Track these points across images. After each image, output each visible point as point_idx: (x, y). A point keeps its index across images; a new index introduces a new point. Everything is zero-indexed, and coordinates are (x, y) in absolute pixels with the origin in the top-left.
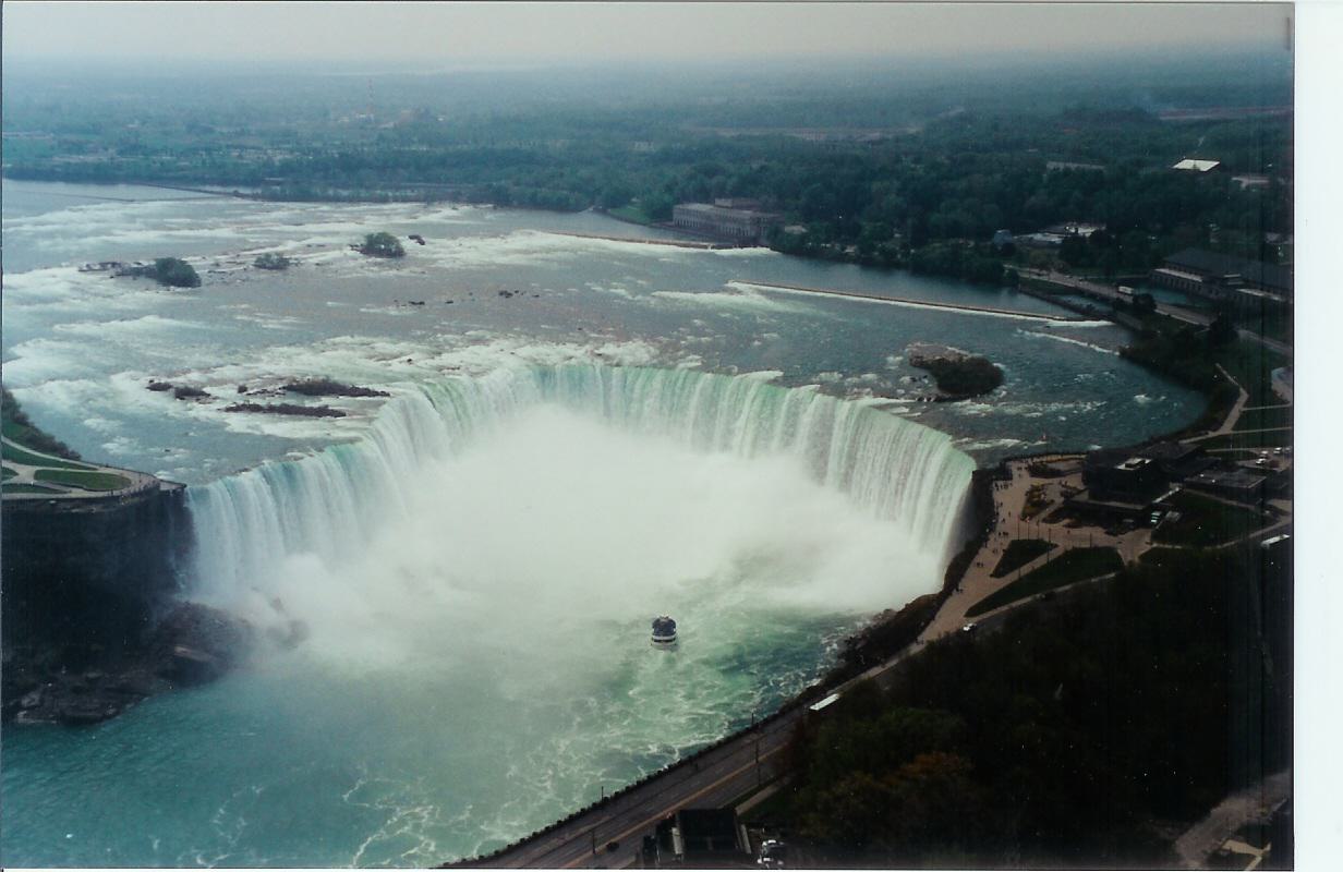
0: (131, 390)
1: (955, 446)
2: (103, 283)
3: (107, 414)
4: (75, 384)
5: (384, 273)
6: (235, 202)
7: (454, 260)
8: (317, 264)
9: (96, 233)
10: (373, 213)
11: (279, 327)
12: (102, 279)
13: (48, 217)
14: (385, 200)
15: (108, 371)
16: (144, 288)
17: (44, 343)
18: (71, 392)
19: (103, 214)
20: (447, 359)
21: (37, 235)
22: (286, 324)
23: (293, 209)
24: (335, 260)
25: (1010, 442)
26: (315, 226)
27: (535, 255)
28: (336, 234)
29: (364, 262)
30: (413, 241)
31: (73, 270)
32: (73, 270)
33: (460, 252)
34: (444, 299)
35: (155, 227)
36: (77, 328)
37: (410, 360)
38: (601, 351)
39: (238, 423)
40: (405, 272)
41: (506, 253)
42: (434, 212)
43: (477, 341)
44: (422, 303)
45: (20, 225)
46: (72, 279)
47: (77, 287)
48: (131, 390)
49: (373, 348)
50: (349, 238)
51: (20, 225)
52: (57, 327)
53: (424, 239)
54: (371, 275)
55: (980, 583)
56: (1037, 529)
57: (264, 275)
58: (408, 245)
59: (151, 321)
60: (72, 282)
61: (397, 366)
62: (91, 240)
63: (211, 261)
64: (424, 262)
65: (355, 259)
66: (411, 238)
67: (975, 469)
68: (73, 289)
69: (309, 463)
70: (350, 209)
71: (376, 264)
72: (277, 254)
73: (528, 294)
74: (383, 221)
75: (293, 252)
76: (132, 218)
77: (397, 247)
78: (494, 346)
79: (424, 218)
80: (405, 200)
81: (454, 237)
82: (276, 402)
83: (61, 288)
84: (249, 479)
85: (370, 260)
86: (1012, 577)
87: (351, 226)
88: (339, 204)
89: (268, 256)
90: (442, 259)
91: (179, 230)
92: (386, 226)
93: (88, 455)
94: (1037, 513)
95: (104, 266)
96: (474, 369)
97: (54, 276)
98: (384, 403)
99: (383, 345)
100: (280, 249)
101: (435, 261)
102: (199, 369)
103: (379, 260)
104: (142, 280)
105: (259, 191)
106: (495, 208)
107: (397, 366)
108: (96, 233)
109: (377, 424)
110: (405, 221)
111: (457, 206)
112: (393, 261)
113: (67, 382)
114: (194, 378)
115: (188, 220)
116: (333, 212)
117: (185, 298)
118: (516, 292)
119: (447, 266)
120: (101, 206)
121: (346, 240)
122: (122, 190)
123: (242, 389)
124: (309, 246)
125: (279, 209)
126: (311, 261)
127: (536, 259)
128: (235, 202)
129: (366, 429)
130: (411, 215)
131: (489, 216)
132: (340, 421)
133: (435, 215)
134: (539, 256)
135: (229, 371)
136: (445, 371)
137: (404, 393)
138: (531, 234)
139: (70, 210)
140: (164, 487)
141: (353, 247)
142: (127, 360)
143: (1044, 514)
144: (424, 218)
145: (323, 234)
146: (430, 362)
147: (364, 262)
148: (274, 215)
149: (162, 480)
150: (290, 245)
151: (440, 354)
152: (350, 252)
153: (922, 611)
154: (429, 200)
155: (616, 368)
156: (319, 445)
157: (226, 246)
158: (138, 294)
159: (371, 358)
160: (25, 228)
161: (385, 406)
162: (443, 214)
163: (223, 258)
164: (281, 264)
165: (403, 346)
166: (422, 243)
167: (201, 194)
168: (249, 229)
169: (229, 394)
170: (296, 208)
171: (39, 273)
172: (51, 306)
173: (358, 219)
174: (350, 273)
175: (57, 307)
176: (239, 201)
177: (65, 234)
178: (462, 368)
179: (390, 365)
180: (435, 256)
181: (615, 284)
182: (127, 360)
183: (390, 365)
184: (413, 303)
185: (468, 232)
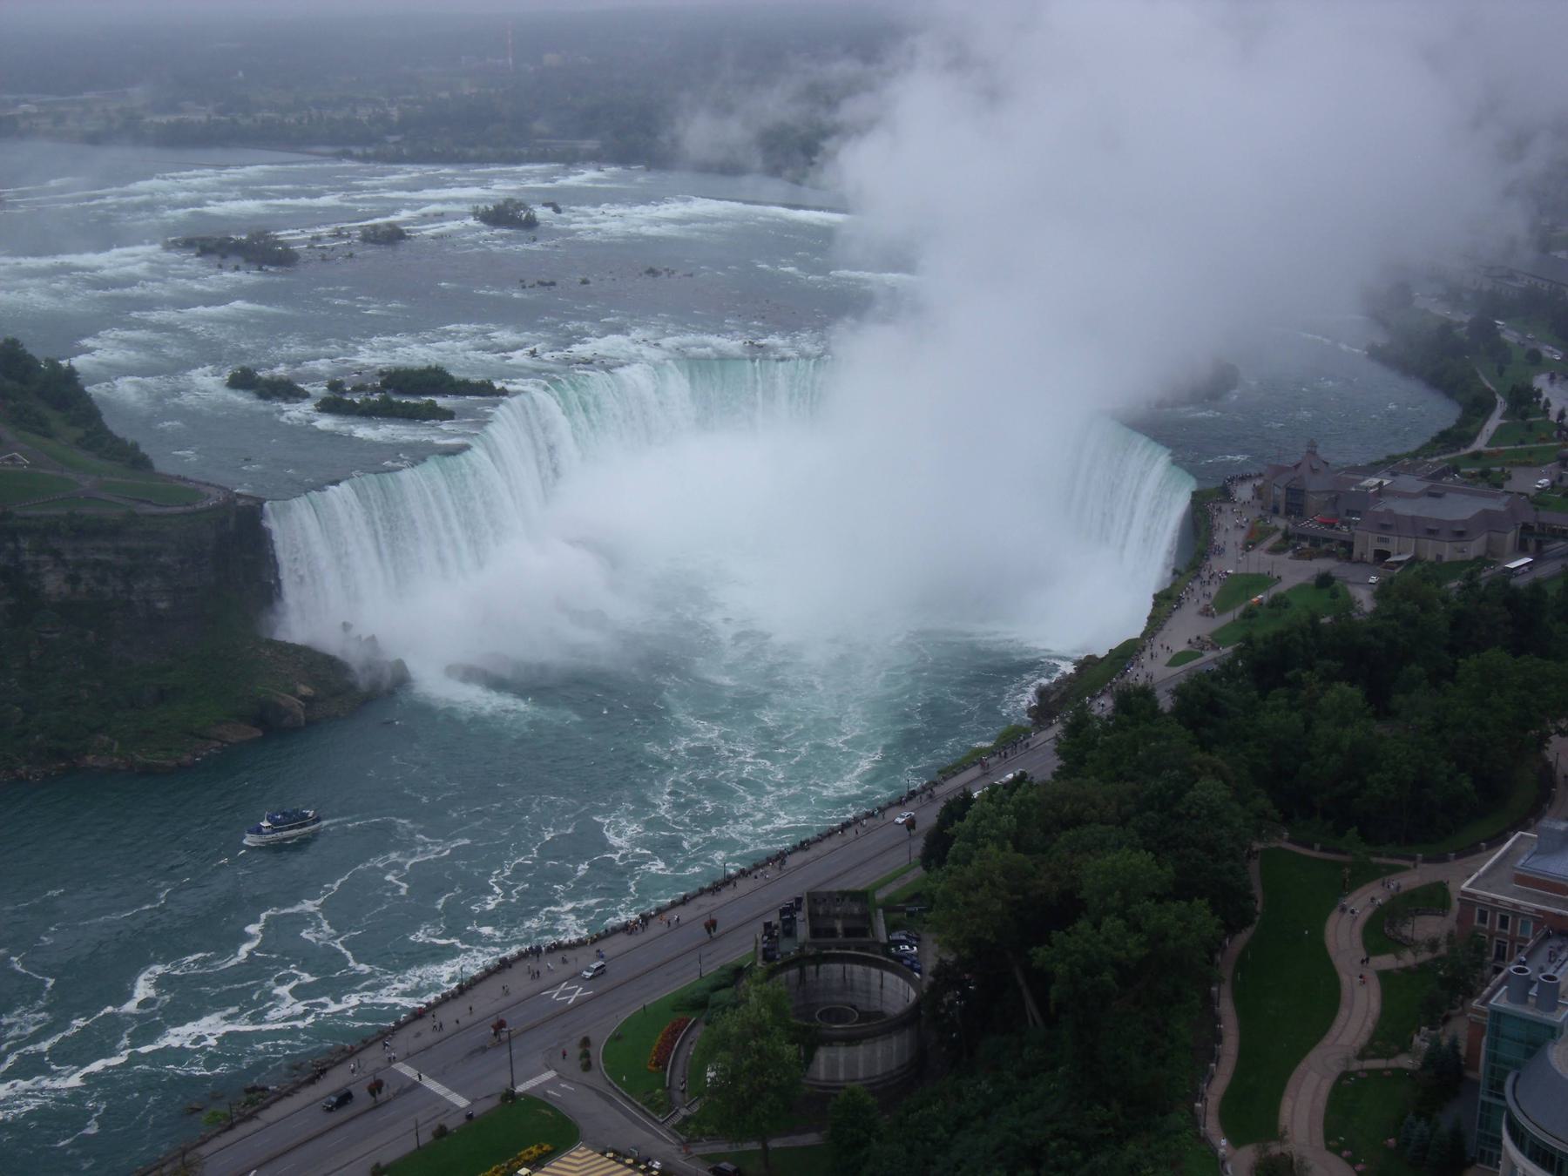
0: (208, 383)
2: (193, 263)
3: (180, 412)
4: (148, 380)
5: (511, 247)
6: (343, 165)
7: (596, 231)
8: (433, 238)
9: (184, 204)
10: (501, 175)
11: (384, 313)
12: (188, 257)
13: (132, 187)
14: (517, 160)
15: (186, 365)
16: (233, 267)
19: (195, 182)
20: (577, 349)
21: (122, 208)
22: (390, 310)
23: (409, 173)
24: (450, 235)
26: (434, 191)
27: (693, 225)
28: (457, 201)
29: (486, 233)
30: (549, 210)
31: (157, 247)
32: (157, 247)
33: (605, 221)
34: (578, 279)
36: (155, 316)
37: (533, 353)
38: (763, 342)
39: (325, 422)
40: (536, 247)
41: (656, 222)
42: (576, 174)
43: (618, 329)
44: (553, 284)
45: (103, 197)
46: (154, 258)
47: (159, 272)
48: (208, 383)
49: (489, 338)
50: (471, 205)
51: (103, 197)
52: (135, 314)
53: (561, 207)
54: (495, 249)
55: (1186, 628)
56: (1260, 561)
57: (371, 250)
58: (542, 213)
60: (153, 261)
61: (519, 357)
62: (181, 212)
63: (309, 234)
64: (559, 233)
65: (478, 230)
66: (546, 205)
67: (1194, 490)
68: (152, 270)
69: (406, 475)
70: (476, 171)
71: (501, 237)
72: (390, 225)
73: (678, 274)
76: (225, 186)
77: (529, 214)
78: (633, 335)
80: (543, 158)
81: (596, 204)
82: (376, 397)
83: (139, 269)
84: (339, 495)
85: (496, 231)
86: (1229, 617)
87: (474, 192)
88: (466, 166)
89: (375, 227)
90: (581, 230)
91: (278, 199)
92: (518, 191)
93: (162, 465)
94: (1261, 540)
95: (188, 244)
96: (607, 362)
97: (134, 255)
98: (501, 402)
99: (504, 336)
100: (392, 219)
101: (573, 232)
102: (288, 363)
103: (506, 231)
104: (234, 260)
105: (370, 151)
106: (648, 170)
107: (519, 357)
108: (184, 205)
109: (490, 428)
111: (603, 166)
112: (522, 233)
113: (140, 379)
114: (281, 371)
115: (298, 187)
116: (461, 176)
117: (278, 279)
118: (667, 270)
119: (588, 238)
120: (195, 172)
121: (465, 208)
122: (217, 154)
123: (335, 386)
124: (425, 215)
125: (394, 173)
126: (424, 233)
127: (696, 230)
128: (343, 165)
129: (477, 434)
130: (547, 177)
131: (641, 179)
132: (446, 426)
134: (699, 225)
135: (322, 365)
136: (574, 366)
137: (523, 392)
138: (688, 200)
139: (158, 178)
140: (241, 502)
141: (476, 214)
142: (209, 353)
143: (1268, 544)
145: (444, 201)
146: (557, 354)
147: (486, 233)
148: (394, 178)
149: (239, 495)
150: (405, 215)
151: (568, 345)
152: (471, 222)
153: (1127, 653)
154: (571, 160)
155: (781, 365)
156: (418, 454)
157: (328, 215)
158: (227, 275)
159: (485, 349)
160: (109, 200)
161: (502, 407)
162: (584, 177)
163: (324, 231)
164: (393, 236)
165: (526, 335)
166: (558, 211)
167: (313, 158)
168: (358, 197)
169: (320, 390)
170: (411, 172)
171: (115, 251)
172: (127, 291)
173: (483, 182)
174: (471, 249)
175: (136, 291)
176: (347, 164)
177: (150, 206)
178: (595, 362)
179: (510, 358)
180: (572, 227)
181: (783, 260)
182: (209, 353)
183: (510, 358)
184: (542, 284)
185: (615, 198)
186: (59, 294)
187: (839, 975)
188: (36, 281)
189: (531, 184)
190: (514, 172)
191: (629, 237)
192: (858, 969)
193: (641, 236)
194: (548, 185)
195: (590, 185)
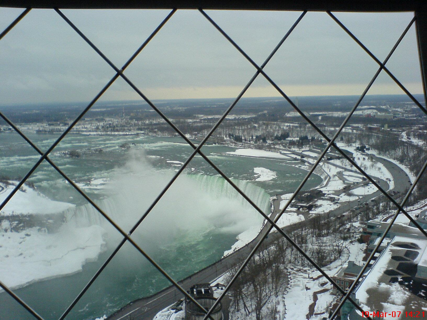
1: (266, 192)
13: (44, 142)
17: (40, 172)
18: (48, 184)
25: (279, 190)
28: (113, 143)
35: (71, 143)
41: (156, 147)
59: (68, 166)
72: (99, 149)
74: (125, 140)
75: (103, 148)
79: (135, 139)
110: (131, 140)
133: (139, 138)
138: (162, 142)
144: (135, 139)
145: (111, 144)
150: (103, 146)
186: (28, 164)
187: (203, 302)
188: (24, 162)
189: (129, 140)
190: (125, 137)
191: (150, 150)
192: (208, 300)
193: (153, 150)
194: (133, 140)
195: (141, 140)
